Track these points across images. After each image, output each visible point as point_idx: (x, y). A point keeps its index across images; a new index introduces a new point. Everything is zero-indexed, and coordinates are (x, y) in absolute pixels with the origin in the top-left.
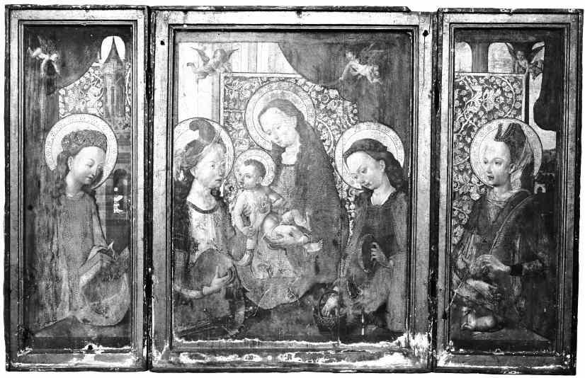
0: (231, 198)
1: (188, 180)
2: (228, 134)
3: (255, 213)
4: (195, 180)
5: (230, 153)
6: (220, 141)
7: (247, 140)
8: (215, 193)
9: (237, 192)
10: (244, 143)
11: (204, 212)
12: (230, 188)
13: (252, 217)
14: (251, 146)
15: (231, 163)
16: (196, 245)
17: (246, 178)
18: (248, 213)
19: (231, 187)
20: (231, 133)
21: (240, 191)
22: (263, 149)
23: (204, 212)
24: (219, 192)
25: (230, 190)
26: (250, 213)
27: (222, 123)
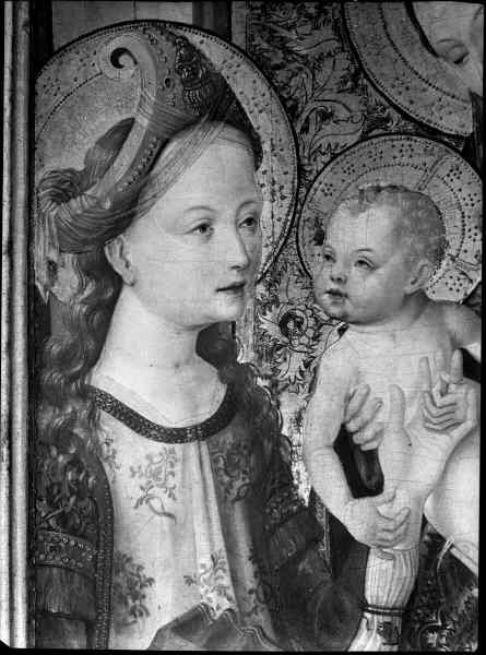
0: (291, 366)
1: (98, 292)
2: (269, 79)
3: (404, 433)
4: (126, 293)
5: (278, 167)
6: (240, 123)
7: (353, 101)
8: (213, 343)
9: (316, 338)
10: (342, 114)
11: (175, 436)
12: (282, 324)
13: (388, 462)
14: (374, 125)
15: (282, 209)
16: (137, 587)
17: (356, 273)
18: (368, 433)
19: (289, 316)
20: (281, 76)
21: (330, 334)
22: (433, 134)
23: (175, 436)
24: (232, 349)
25: (285, 332)
26: (378, 435)
27: (239, 38)
